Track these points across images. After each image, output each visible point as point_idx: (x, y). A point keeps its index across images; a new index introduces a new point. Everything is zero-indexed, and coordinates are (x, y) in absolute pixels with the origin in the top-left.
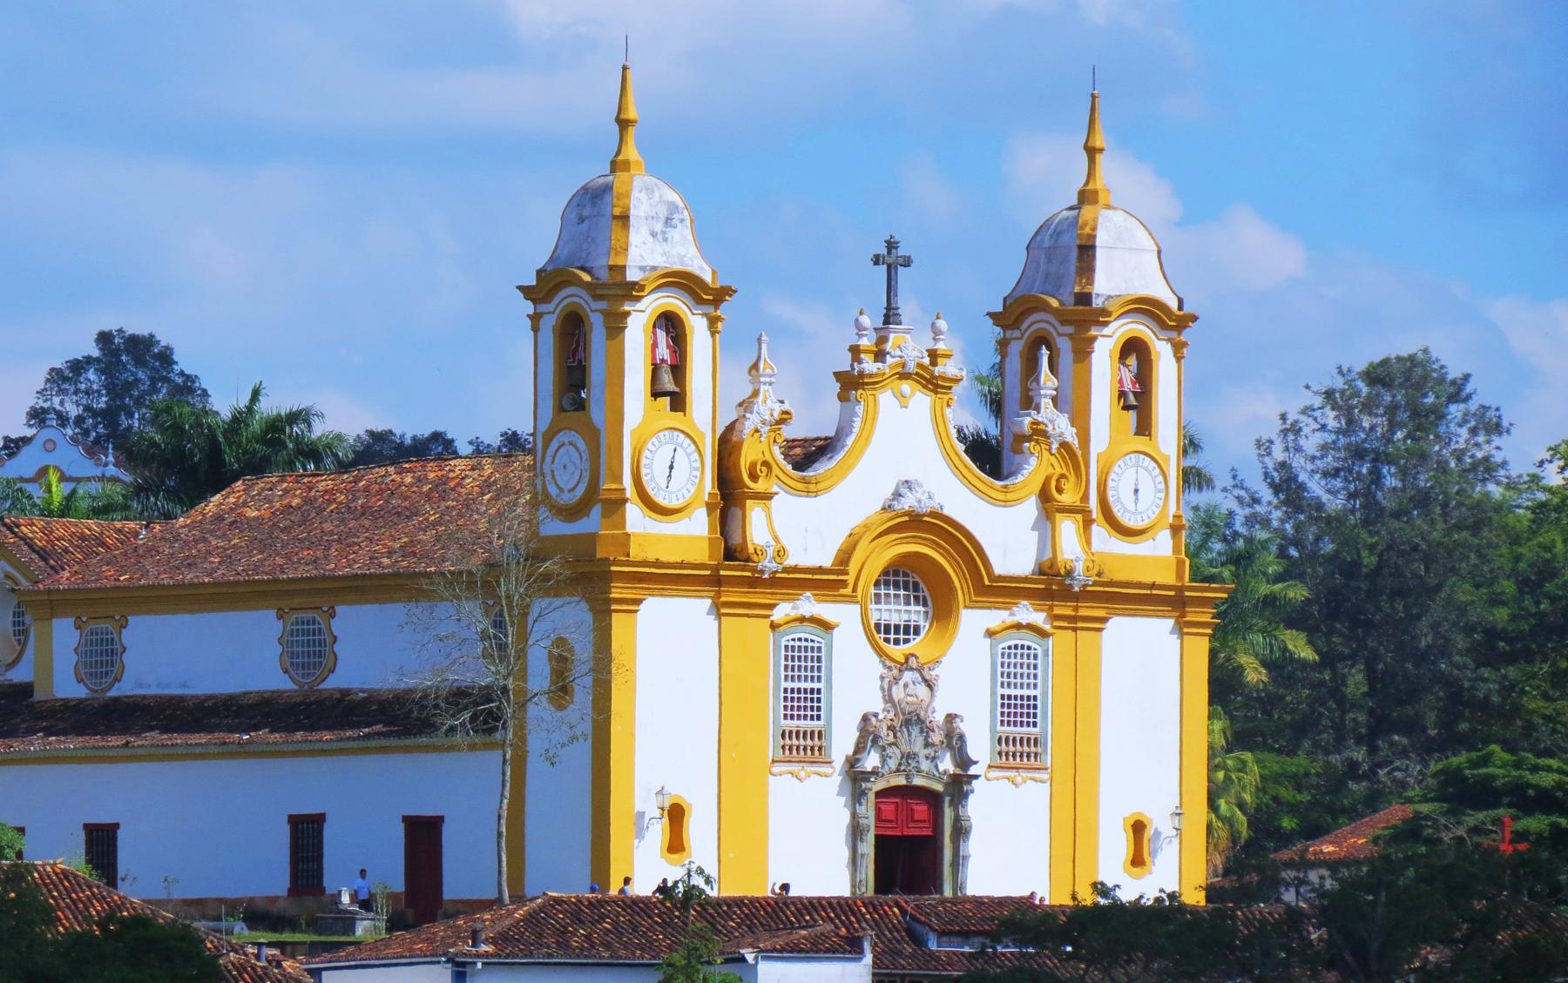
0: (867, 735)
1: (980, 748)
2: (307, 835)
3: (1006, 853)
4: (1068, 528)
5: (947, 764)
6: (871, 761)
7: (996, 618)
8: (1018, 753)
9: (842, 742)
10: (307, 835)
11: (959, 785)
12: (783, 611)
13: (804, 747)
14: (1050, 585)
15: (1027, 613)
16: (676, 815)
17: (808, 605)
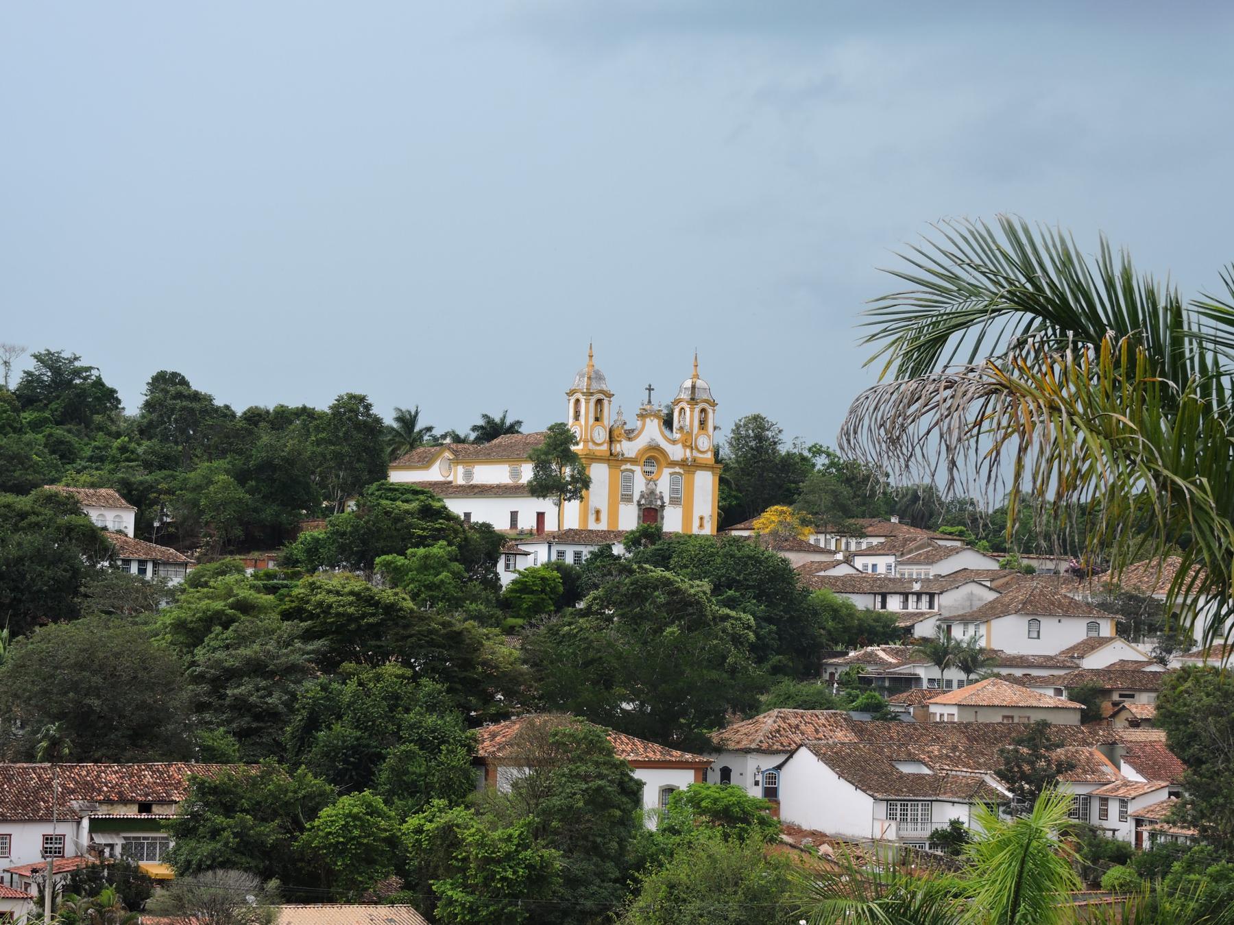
0: (642, 496)
1: (666, 500)
2: (514, 515)
3: (672, 522)
4: (688, 451)
5: (659, 503)
6: (643, 502)
7: (672, 470)
8: (675, 501)
9: (636, 497)
10: (514, 515)
11: (663, 507)
12: (623, 467)
13: (628, 498)
14: (683, 463)
15: (677, 469)
16: (598, 512)
17: (628, 466)
